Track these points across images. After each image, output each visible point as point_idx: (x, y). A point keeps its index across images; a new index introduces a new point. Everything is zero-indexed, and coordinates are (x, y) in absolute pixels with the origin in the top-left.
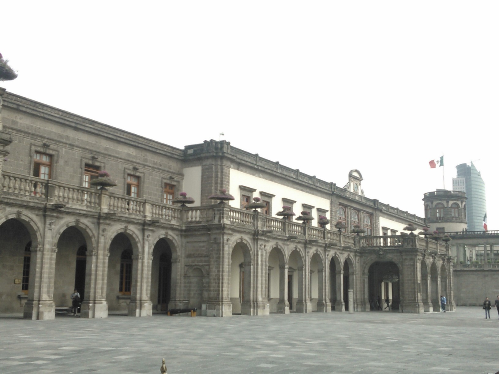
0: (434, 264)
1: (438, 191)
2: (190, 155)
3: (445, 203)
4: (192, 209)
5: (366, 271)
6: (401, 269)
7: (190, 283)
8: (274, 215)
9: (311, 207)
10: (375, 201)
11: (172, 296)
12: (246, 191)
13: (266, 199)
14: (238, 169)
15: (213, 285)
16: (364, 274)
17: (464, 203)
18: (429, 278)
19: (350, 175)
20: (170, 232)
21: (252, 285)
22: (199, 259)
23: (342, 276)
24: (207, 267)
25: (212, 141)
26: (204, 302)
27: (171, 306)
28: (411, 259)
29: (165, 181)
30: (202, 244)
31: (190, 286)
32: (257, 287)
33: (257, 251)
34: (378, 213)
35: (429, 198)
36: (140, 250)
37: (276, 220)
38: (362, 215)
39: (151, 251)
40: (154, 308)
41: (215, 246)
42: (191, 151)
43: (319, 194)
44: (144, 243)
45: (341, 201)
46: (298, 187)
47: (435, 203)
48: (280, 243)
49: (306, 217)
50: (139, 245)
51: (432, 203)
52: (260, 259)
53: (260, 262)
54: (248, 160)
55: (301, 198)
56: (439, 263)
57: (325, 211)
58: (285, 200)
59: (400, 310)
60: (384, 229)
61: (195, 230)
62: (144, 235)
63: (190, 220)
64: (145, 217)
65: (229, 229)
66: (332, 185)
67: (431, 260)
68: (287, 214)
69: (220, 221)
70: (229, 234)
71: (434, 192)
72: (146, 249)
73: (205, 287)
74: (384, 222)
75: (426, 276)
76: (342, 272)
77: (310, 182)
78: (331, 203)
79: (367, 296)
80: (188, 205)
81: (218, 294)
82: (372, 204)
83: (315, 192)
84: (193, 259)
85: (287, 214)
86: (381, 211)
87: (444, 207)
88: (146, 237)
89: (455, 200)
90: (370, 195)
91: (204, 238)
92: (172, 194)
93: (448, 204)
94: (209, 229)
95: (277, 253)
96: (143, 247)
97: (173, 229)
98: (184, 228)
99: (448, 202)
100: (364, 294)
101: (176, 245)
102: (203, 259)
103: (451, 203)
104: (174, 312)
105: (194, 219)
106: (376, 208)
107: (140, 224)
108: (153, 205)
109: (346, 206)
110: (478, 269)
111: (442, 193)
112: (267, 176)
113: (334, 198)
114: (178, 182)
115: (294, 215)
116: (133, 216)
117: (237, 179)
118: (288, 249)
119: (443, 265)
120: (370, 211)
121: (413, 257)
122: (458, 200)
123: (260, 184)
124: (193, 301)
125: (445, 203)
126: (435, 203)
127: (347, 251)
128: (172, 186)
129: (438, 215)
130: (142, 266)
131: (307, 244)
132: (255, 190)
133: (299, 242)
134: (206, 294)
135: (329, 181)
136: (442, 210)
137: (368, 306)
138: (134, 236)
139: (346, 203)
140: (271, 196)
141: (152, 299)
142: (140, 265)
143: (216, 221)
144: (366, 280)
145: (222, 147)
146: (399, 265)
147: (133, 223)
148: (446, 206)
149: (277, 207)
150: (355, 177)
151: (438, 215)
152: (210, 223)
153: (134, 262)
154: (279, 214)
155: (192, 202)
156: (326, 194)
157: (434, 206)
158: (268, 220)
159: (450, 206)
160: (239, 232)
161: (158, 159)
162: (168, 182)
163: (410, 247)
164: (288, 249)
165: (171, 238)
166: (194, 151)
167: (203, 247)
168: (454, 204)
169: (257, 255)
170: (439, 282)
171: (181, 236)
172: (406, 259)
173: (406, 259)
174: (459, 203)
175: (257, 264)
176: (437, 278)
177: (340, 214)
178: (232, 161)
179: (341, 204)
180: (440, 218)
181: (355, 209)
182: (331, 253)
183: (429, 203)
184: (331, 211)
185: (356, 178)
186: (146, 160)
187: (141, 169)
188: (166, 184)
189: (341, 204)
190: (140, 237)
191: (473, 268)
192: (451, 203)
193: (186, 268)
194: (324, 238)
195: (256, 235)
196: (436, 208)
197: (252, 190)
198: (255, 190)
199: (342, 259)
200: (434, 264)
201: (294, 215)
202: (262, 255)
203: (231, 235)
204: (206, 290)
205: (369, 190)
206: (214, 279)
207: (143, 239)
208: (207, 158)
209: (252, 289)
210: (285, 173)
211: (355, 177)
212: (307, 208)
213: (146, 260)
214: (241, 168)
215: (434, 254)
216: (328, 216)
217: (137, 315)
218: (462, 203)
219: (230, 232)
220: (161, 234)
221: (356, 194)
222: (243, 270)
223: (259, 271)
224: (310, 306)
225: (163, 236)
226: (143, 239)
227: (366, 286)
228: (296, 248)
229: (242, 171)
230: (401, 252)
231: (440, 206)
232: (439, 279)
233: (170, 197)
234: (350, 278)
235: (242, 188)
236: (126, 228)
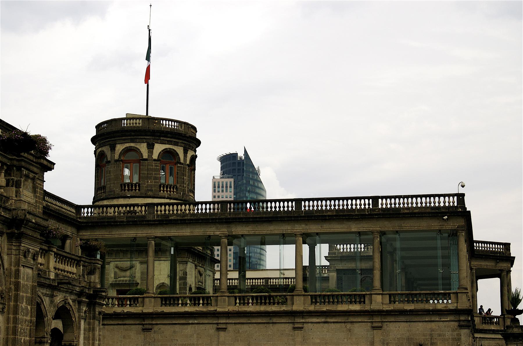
1: (130, 118)
3: (143, 148)
17: (190, 153)
47: (120, 148)
51: (113, 149)
71: (121, 119)
87: (141, 160)
89: (169, 143)
93: (151, 152)
99: (151, 147)
122: (176, 144)
125: (143, 148)
126: (120, 148)
148: (145, 155)
157: (117, 157)
159: (155, 156)
168: (166, 153)
174: (180, 151)
180: (130, 185)
183: (106, 149)
191: (188, 309)
192: (159, 148)
218: (185, 152)
231: (130, 156)
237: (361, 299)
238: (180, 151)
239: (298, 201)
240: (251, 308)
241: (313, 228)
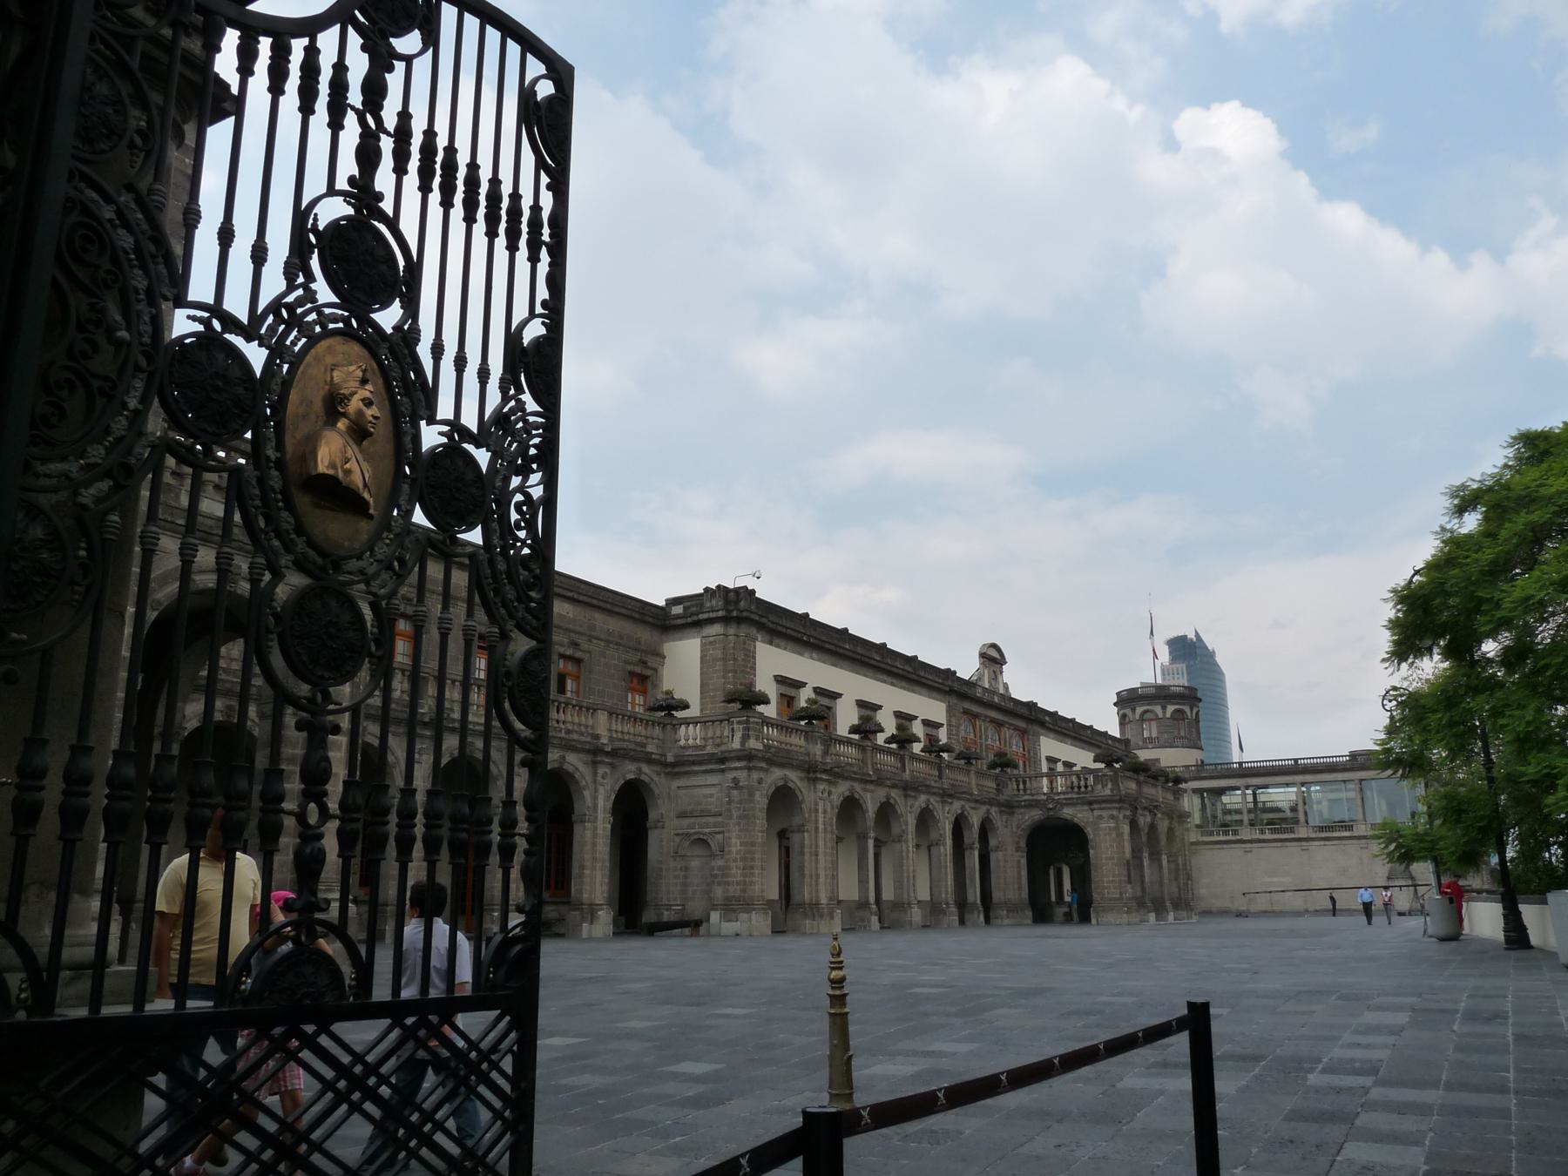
0: (1152, 827)
1: (1145, 686)
2: (678, 617)
3: (1158, 709)
4: (687, 722)
5: (1023, 844)
6: (1091, 837)
7: (687, 868)
8: (842, 730)
9: (912, 718)
10: (1031, 706)
11: (649, 898)
12: (788, 684)
13: (825, 701)
14: (771, 644)
15: (736, 873)
16: (1018, 849)
18: (1146, 855)
19: (983, 655)
20: (645, 768)
21: (807, 872)
22: (704, 820)
23: (976, 853)
24: (720, 837)
25: (719, 587)
26: (714, 907)
27: (649, 916)
28: (1112, 817)
29: (630, 668)
30: (707, 791)
31: (686, 877)
32: (818, 876)
33: (816, 804)
34: (1036, 728)
35: (1127, 700)
36: (589, 802)
37: (849, 742)
38: (1007, 732)
39: (610, 805)
40: (615, 923)
41: (735, 792)
42: (677, 610)
43: (924, 691)
44: (596, 790)
45: (967, 705)
46: (884, 677)
47: (1139, 710)
48: (857, 786)
49: (903, 739)
50: (586, 793)
51: (1134, 710)
52: (821, 820)
53: (821, 826)
54: (789, 624)
55: (892, 699)
56: (1163, 825)
57: (938, 726)
58: (862, 704)
59: (1094, 921)
60: (1051, 760)
61: (694, 763)
62: (595, 774)
63: (682, 743)
64: (597, 737)
65: (763, 759)
66: (949, 674)
67: (1149, 819)
68: (867, 728)
69: (743, 743)
70: (761, 769)
72: (601, 802)
73: (716, 876)
74: (1050, 746)
75: (1140, 851)
76: (977, 845)
77: (908, 668)
78: (950, 710)
79: (1025, 894)
80: (679, 714)
81: (744, 891)
82: (1024, 711)
83: (917, 688)
84: (693, 820)
85: (867, 728)
86: (1042, 724)
87: (1157, 719)
88: (599, 779)
90: (1020, 693)
91: (713, 779)
92: (644, 693)
94: (722, 761)
95: (850, 807)
96: (595, 798)
97: (649, 760)
98: (670, 759)
99: (1164, 708)
100: (1020, 888)
101: (657, 792)
102: (711, 820)
103: (1171, 709)
104: (654, 929)
105: (691, 742)
106: (1034, 718)
107: (588, 751)
108: (611, 714)
109: (975, 716)
110: (1231, 837)
111: (1153, 691)
112: (826, 657)
113: (954, 700)
114: (656, 670)
115: (882, 730)
116: (575, 736)
117: (772, 663)
118: (871, 802)
119: (1171, 830)
120: (1021, 724)
121: (1115, 812)
123: (814, 672)
124: (695, 909)
126: (1139, 710)
127: (984, 803)
128: (643, 679)
129: (1146, 734)
130: (595, 836)
131: (910, 788)
132: (804, 684)
133: (894, 786)
134: (718, 892)
135: (942, 667)
136: (1154, 724)
137: (1029, 913)
138: (577, 775)
139: (975, 709)
140: (835, 696)
141: (610, 903)
142: (588, 833)
143: (736, 745)
144: (1024, 861)
145: (738, 601)
146: (1089, 830)
147: (574, 749)
149: (846, 718)
150: (993, 658)
151: (1146, 734)
152: (723, 748)
153: (577, 829)
154: (854, 730)
155: (686, 706)
156: (939, 690)
158: (832, 740)
160: (781, 765)
161: (615, 625)
162: (638, 669)
163: (1107, 792)
164: (871, 802)
165: (646, 779)
166: (685, 609)
167: (712, 795)
169: (817, 811)
170: (1165, 863)
171: (667, 774)
172: (1100, 817)
173: (1100, 817)
174: (1187, 709)
175: (817, 829)
176: (1159, 854)
177: (966, 730)
178: (761, 627)
179: (966, 712)
180: (1150, 738)
181: (993, 721)
182: (957, 806)
183: (1128, 711)
184: (949, 725)
185: (992, 660)
186: (592, 628)
187: (584, 645)
188: (632, 674)
189: (966, 712)
190: (589, 778)
191: (1222, 838)
192: (1171, 709)
193: (677, 839)
194: (940, 777)
195: (811, 771)
196: (1142, 720)
197: (799, 685)
198: (804, 684)
199: (975, 820)
200: (1152, 827)
201: (882, 730)
202: (825, 812)
203: (767, 770)
204: (719, 884)
205: (1020, 684)
206: (735, 860)
207: (595, 781)
208: (711, 621)
209: (807, 880)
210: (859, 650)
211: (993, 658)
212: (904, 718)
213: (600, 825)
214: (776, 641)
215: (1152, 809)
216: (943, 736)
217: (585, 934)
219: (763, 765)
220: (629, 770)
221: (994, 692)
222: (785, 842)
223: (821, 843)
224: (916, 914)
225: (630, 776)
226: (595, 781)
227: (1024, 873)
228: (888, 797)
229: (778, 646)
230: (1090, 803)
232: (1164, 857)
233: (639, 699)
234: (993, 856)
235: (781, 680)
236: (563, 757)
237: (1350, 828)
238: (1187, 709)
239: (1296, 760)
240: (1268, 836)
241: (1309, 778)
